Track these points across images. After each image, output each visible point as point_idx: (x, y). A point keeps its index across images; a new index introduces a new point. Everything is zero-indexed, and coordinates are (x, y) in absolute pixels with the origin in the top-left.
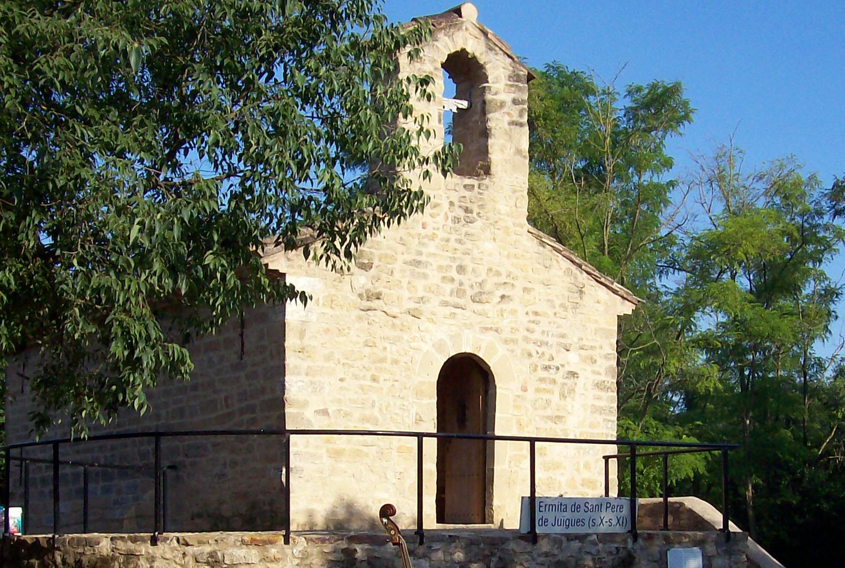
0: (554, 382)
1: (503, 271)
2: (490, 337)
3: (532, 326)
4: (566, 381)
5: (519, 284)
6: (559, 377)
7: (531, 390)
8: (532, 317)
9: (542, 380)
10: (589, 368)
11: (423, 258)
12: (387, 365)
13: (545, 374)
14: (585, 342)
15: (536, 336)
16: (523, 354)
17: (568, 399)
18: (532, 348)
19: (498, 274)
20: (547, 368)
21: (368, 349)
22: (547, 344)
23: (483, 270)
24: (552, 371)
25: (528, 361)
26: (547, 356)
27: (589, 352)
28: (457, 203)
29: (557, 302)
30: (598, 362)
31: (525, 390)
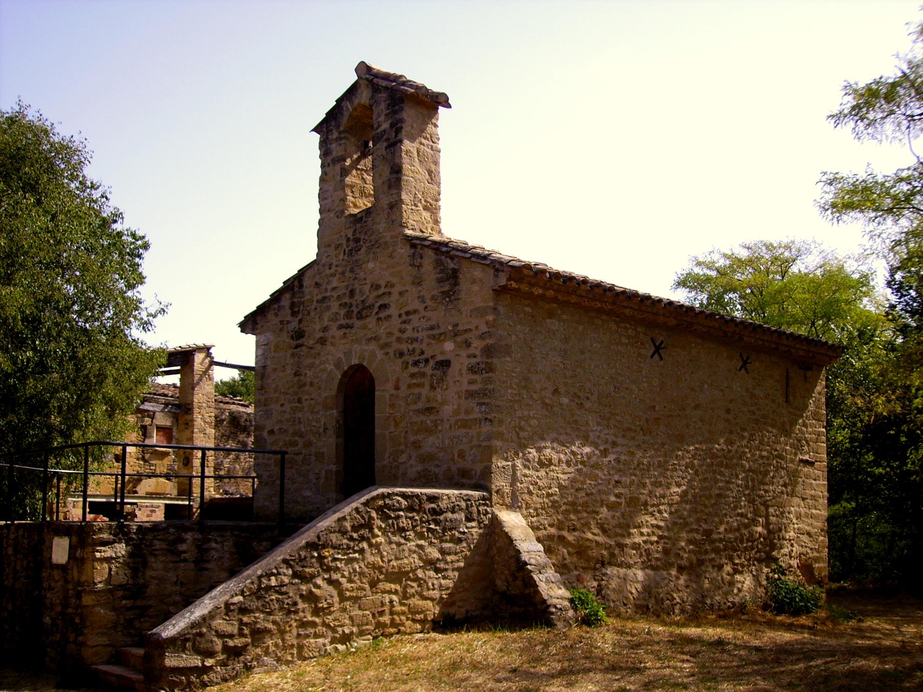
0: (423, 375)
1: (383, 284)
2: (373, 346)
3: (404, 326)
4: (435, 372)
5: (395, 291)
6: (428, 370)
7: (403, 387)
8: (404, 317)
9: (413, 376)
10: (464, 354)
11: (328, 294)
12: (307, 388)
13: (415, 370)
14: (460, 328)
15: (409, 334)
16: (395, 355)
17: (438, 390)
18: (404, 347)
19: (378, 287)
20: (416, 363)
21: (297, 378)
22: (416, 340)
23: (367, 288)
24: (422, 365)
25: (399, 361)
26: (418, 351)
27: (466, 336)
28: (352, 238)
29: (428, 297)
30: (473, 345)
31: (397, 388)
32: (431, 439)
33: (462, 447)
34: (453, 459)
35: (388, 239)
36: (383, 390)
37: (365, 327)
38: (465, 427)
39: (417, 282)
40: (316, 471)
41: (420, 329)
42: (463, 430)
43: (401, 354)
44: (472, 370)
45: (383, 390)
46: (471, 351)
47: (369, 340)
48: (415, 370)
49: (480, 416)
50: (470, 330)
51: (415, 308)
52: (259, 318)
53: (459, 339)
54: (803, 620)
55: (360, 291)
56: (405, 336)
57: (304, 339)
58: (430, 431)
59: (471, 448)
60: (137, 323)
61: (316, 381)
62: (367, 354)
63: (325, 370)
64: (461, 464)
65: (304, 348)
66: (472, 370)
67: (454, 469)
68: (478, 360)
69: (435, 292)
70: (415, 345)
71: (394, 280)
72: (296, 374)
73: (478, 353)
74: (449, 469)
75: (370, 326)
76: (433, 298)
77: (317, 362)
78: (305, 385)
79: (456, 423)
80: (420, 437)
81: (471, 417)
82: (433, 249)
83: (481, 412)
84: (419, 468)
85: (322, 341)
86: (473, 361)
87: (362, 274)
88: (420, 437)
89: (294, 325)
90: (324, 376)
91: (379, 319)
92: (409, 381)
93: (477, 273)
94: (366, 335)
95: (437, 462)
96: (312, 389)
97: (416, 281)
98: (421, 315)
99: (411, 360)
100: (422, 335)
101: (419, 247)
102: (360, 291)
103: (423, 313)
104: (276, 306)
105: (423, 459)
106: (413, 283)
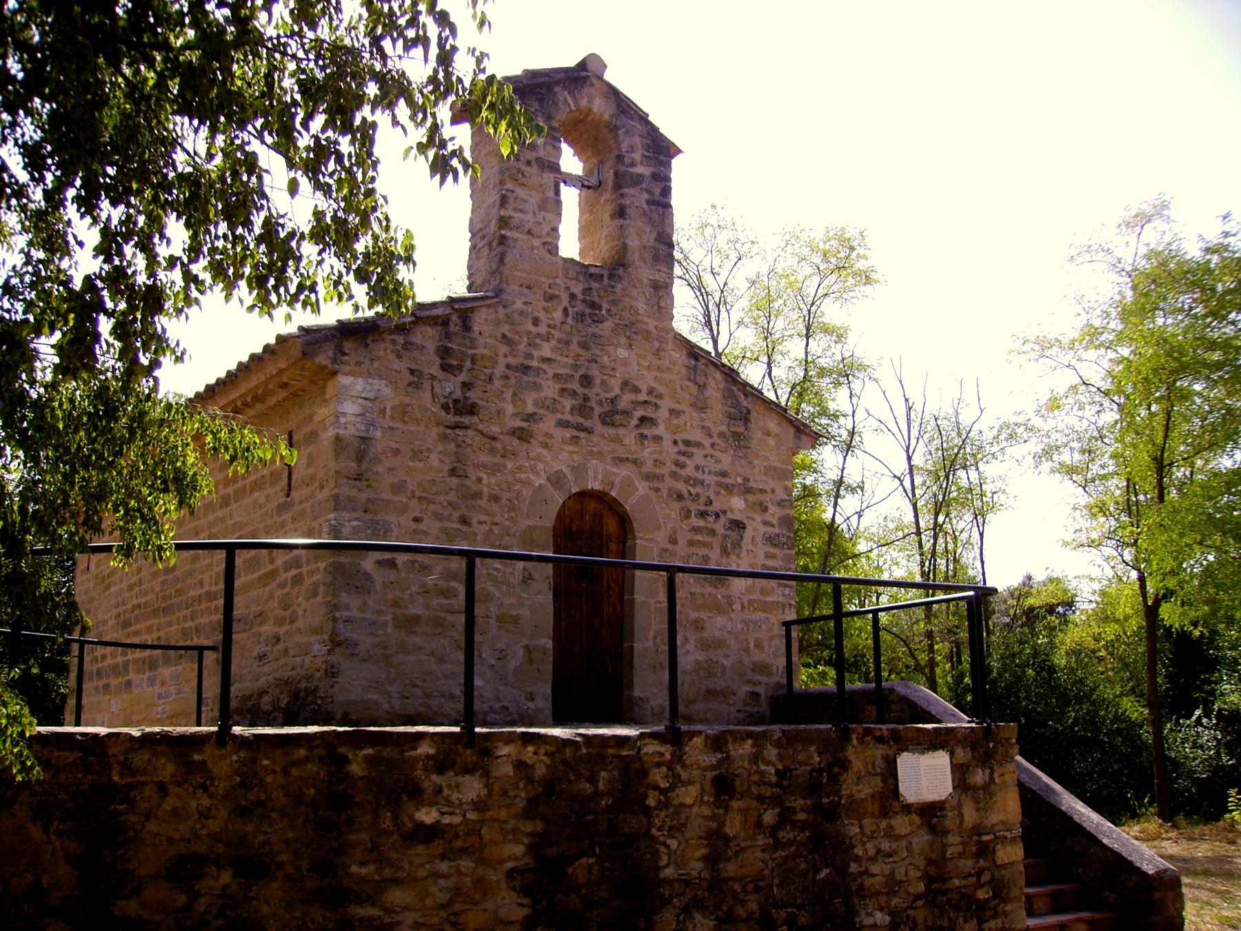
0: (713, 532)
1: (644, 388)
2: (625, 471)
3: (682, 459)
4: (728, 533)
5: (666, 404)
6: (719, 527)
7: (682, 542)
8: (682, 447)
9: (696, 530)
10: (759, 518)
11: (534, 363)
12: (483, 503)
13: (701, 523)
14: (751, 484)
15: (689, 471)
16: (670, 495)
17: (733, 557)
18: (683, 488)
19: (636, 390)
20: (703, 515)
21: (455, 481)
22: (702, 482)
23: (615, 384)
24: (711, 519)
25: (676, 506)
26: (703, 499)
27: (760, 497)
28: (580, 297)
29: (715, 431)
30: (771, 511)
31: (673, 541)
32: (720, 620)
33: (759, 635)
34: (747, 650)
35: (651, 328)
36: (650, 540)
37: (618, 440)
38: (764, 610)
39: (701, 406)
40: (500, 645)
41: (707, 470)
42: (762, 615)
43: (680, 497)
44: (771, 540)
45: (650, 540)
46: (767, 517)
47: (621, 460)
48: (701, 523)
49: (781, 599)
50: (766, 491)
51: (699, 439)
52: (348, 346)
53: (750, 498)
54: (510, 865)
55: (603, 383)
56: (683, 472)
57: (475, 419)
58: (719, 609)
59: (772, 638)
60: (639, 337)
61: (507, 495)
62: (617, 481)
63: (527, 483)
64: (758, 657)
65: (471, 433)
66: (771, 540)
67: (746, 660)
68: (777, 530)
69: (724, 428)
70: (698, 489)
71: (661, 389)
72: (453, 472)
73: (775, 522)
74: (740, 662)
75: (626, 441)
76: (721, 435)
77: (510, 465)
78: (477, 495)
79: (750, 602)
80: (704, 615)
81: (769, 599)
82: (722, 372)
83: (783, 595)
84: (700, 657)
85: (523, 435)
86: (769, 529)
87: (606, 359)
88: (704, 615)
89: (451, 386)
90: (527, 493)
91: (643, 437)
92: (690, 536)
93: (772, 424)
94: (613, 451)
95: (725, 651)
96: (494, 507)
97: (700, 405)
98: (705, 452)
99: (694, 507)
100: (708, 479)
101: (703, 361)
102: (603, 383)
103: (709, 451)
104: (400, 340)
105: (705, 645)
106: (694, 405)
